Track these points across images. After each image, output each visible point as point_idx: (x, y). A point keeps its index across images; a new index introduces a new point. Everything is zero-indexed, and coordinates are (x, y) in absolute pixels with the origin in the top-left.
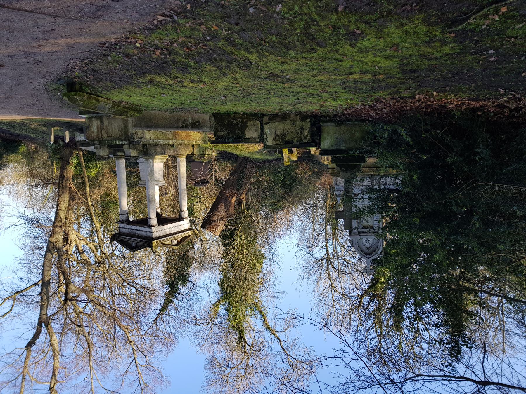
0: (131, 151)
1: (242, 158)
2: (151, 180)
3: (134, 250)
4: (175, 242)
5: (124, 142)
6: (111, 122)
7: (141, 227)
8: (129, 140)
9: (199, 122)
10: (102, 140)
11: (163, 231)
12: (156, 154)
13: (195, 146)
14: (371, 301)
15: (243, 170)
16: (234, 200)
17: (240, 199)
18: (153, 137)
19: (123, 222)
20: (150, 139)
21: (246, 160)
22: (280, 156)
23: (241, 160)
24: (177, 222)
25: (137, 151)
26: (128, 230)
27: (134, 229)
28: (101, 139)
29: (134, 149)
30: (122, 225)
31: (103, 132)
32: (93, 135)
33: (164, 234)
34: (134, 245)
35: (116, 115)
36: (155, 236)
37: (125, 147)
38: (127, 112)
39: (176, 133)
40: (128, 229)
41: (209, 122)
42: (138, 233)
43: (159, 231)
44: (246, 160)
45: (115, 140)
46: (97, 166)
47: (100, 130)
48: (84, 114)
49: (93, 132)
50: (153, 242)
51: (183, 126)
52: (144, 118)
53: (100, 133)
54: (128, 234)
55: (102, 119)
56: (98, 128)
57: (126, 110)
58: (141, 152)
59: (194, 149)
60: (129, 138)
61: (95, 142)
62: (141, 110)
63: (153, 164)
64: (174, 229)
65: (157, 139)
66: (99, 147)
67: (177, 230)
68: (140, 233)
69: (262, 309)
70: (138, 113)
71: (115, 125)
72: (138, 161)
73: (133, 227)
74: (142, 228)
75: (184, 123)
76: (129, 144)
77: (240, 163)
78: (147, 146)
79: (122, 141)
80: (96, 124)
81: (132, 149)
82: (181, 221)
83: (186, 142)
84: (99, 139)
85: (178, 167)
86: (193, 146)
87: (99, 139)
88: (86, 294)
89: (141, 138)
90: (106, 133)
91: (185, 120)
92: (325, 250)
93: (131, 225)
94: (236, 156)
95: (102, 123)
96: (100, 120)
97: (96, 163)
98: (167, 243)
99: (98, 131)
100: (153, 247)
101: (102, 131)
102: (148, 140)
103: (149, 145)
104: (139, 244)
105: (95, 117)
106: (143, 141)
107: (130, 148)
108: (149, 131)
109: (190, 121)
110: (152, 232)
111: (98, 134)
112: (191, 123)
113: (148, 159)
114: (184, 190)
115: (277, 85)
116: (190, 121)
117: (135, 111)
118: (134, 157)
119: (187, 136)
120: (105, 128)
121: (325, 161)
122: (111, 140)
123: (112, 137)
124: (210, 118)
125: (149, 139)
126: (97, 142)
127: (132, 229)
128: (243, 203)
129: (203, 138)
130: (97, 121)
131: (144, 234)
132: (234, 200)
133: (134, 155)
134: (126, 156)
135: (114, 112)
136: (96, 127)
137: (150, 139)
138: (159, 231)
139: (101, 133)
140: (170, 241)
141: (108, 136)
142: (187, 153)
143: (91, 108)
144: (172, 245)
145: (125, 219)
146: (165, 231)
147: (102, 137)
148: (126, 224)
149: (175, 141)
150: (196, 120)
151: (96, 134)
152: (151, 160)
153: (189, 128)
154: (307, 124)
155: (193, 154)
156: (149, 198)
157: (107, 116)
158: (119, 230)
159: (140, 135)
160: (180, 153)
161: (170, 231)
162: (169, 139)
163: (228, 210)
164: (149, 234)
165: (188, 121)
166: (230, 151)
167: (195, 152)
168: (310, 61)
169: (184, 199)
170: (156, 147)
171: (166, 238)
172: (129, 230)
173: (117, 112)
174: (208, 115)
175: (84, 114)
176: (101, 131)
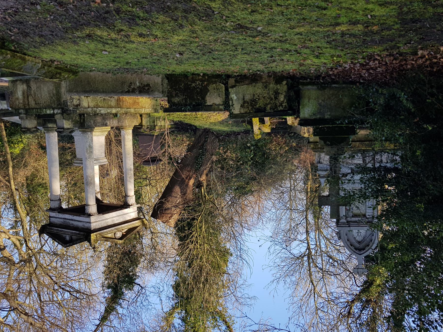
0: (64, 121)
1: (202, 131)
2: (89, 158)
3: (68, 245)
4: (119, 235)
5: (56, 111)
6: (40, 86)
7: (77, 216)
8: (62, 109)
9: (148, 85)
10: (29, 109)
11: (104, 221)
12: (96, 126)
13: (144, 116)
14: (363, 308)
15: (203, 145)
16: (192, 182)
17: (199, 181)
18: (91, 105)
19: (55, 210)
20: (89, 107)
21: (207, 132)
22: (249, 127)
23: (200, 133)
24: (121, 209)
25: (72, 121)
26: (60, 220)
27: (68, 219)
29: (68, 120)
30: (53, 214)
33: (105, 225)
34: (68, 238)
35: (46, 77)
36: (94, 228)
37: (57, 117)
38: (60, 74)
39: (120, 99)
40: (61, 218)
41: (161, 86)
42: (72, 224)
43: (99, 221)
44: (207, 132)
46: (22, 141)
47: (26, 97)
48: (6, 77)
50: (92, 235)
51: (129, 90)
52: (81, 81)
53: (26, 100)
54: (60, 225)
55: (29, 83)
56: (23, 93)
57: (59, 71)
58: (77, 123)
59: (143, 119)
60: (63, 106)
62: (77, 71)
63: (92, 138)
64: (117, 218)
65: (97, 106)
66: (25, 118)
67: (121, 220)
68: (76, 223)
69: (227, 319)
70: (73, 75)
71: (45, 89)
72: (73, 134)
73: (67, 216)
74: (78, 217)
75: (130, 86)
76: (62, 114)
77: (200, 136)
78: (84, 116)
79: (54, 109)
80: (21, 89)
81: (66, 119)
82: (126, 208)
83: (132, 110)
84: (25, 107)
85: (122, 141)
86: (141, 116)
87: (25, 107)
88: (8, 300)
89: (77, 105)
90: (34, 100)
91: (131, 83)
92: (306, 245)
93: (64, 214)
94: (194, 128)
95: (29, 87)
96: (27, 84)
97: (21, 137)
98: (109, 235)
99: (24, 97)
100: (92, 241)
101: (29, 98)
102: (86, 108)
103: (87, 114)
104: (74, 237)
105: (21, 80)
106: (80, 109)
107: (63, 118)
108: (87, 97)
109: (138, 84)
110: (90, 223)
111: (24, 101)
112: (140, 86)
113: (85, 132)
114: (131, 170)
115: (245, 39)
116: (138, 84)
117: (69, 72)
118: (68, 129)
119: (134, 103)
120: (32, 93)
121: (305, 133)
122: (40, 109)
123: (41, 105)
124: (162, 81)
125: (87, 107)
126: (22, 111)
127: (65, 219)
128: (203, 186)
129: (153, 105)
130: (23, 84)
131: (80, 225)
132: (192, 182)
133: (69, 127)
134: (58, 129)
135: (45, 74)
136: (21, 92)
137: (89, 107)
138: (99, 221)
139: (28, 101)
140: (113, 234)
141: (36, 104)
142: (134, 125)
143: (16, 69)
144: (116, 239)
145: (57, 206)
146: (107, 221)
147: (28, 105)
148: (59, 212)
149: (120, 109)
150: (146, 84)
151: (21, 102)
152: (89, 133)
153: (137, 93)
154: (283, 87)
155: (141, 125)
156: (86, 180)
157: (35, 79)
158: (50, 220)
159: (75, 102)
160: (125, 124)
161: (113, 221)
162: (112, 107)
163: (184, 194)
164: (87, 225)
165: (135, 84)
166: (187, 121)
167: (144, 123)
168: (287, 9)
169: (130, 182)
170: (95, 117)
171: (108, 230)
172: (62, 220)
173: (48, 74)
174: (161, 76)
175: (7, 76)
176: (28, 97)
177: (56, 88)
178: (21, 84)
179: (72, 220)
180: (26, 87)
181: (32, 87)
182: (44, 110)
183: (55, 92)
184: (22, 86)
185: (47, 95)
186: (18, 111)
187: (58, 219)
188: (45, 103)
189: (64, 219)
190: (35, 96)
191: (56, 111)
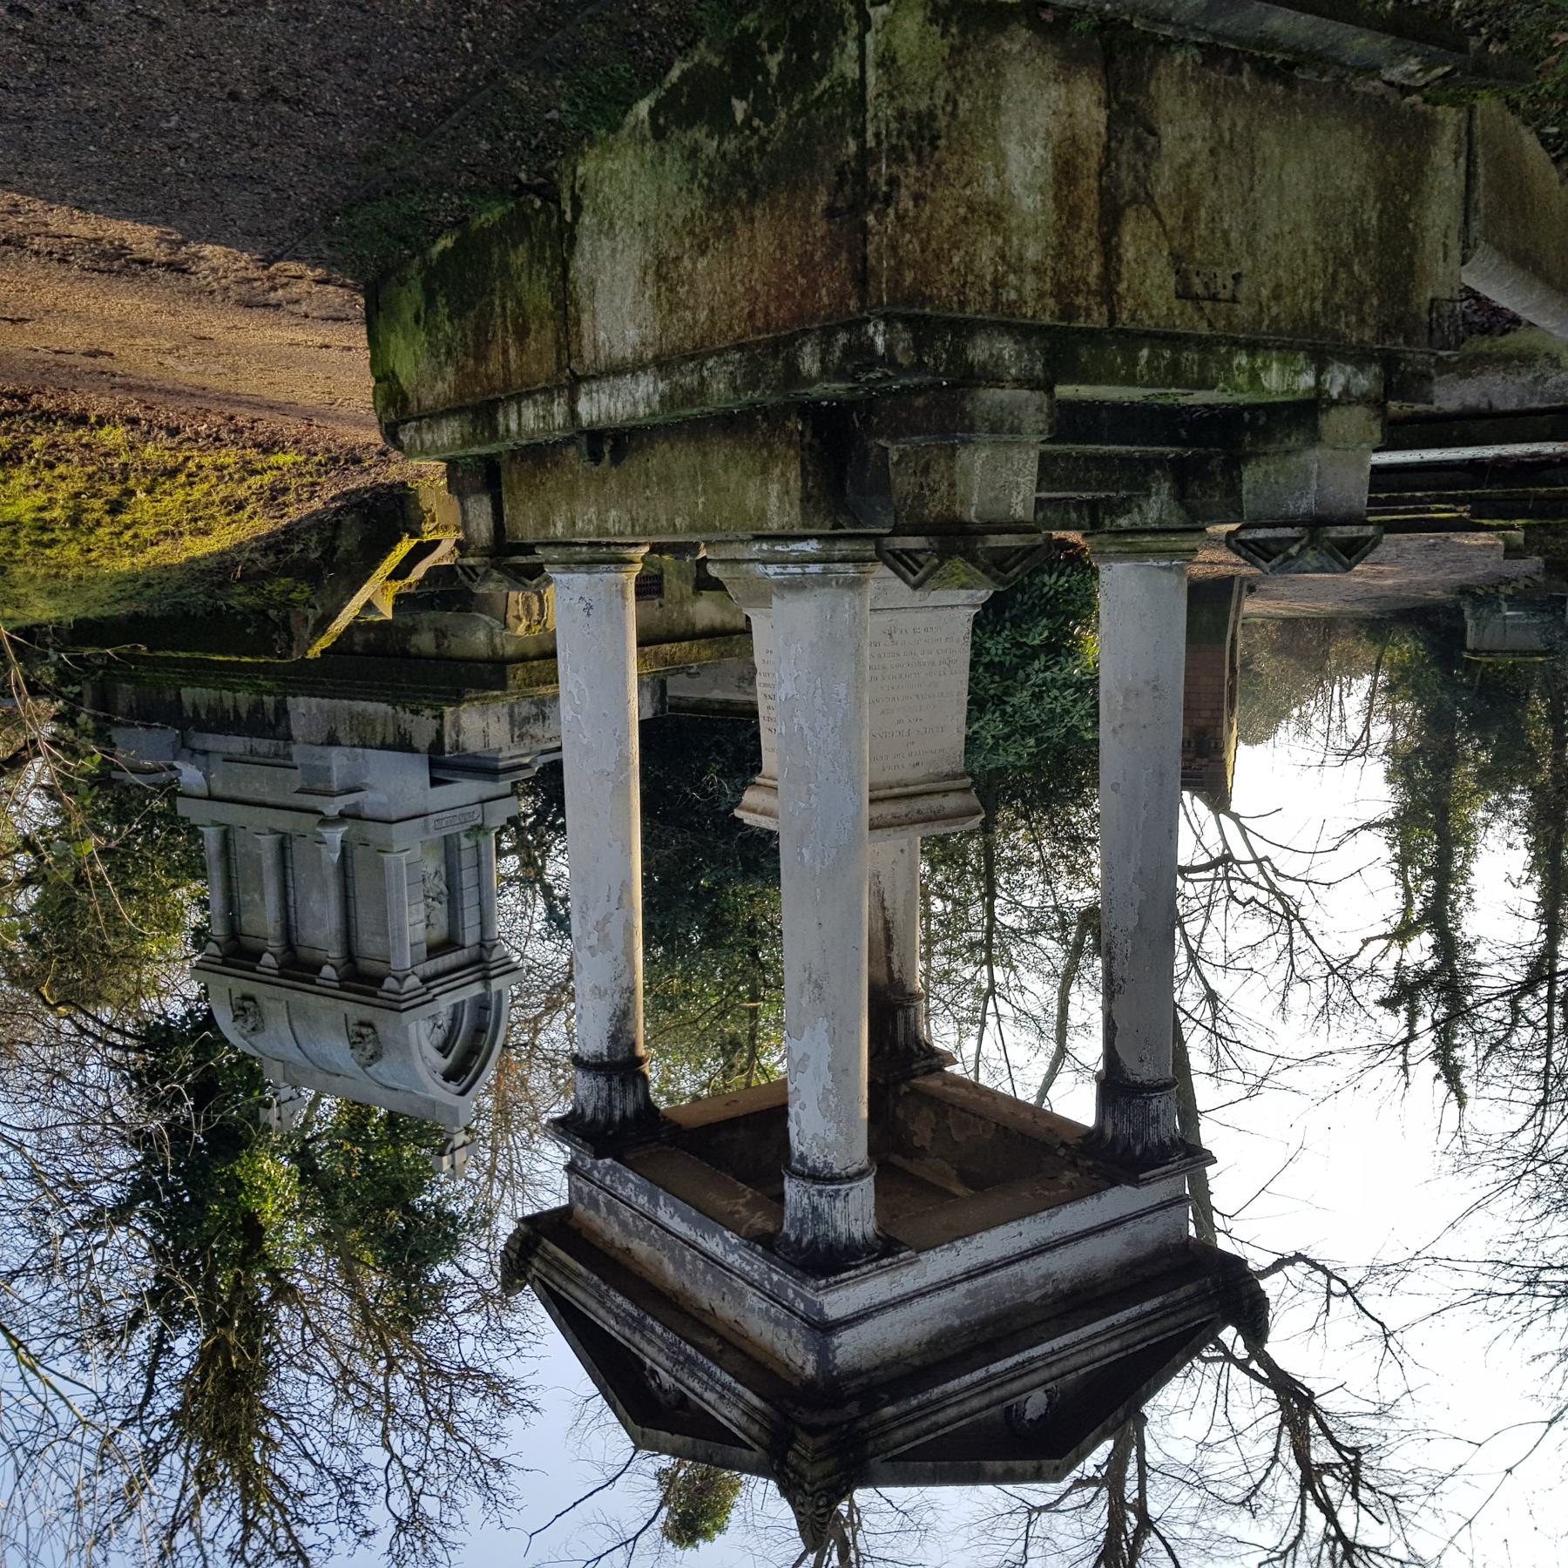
28: (1099, 319)
31: (1134, 238)
32: (986, 255)
45: (1252, 348)
47: (1091, 207)
49: (994, 215)
53: (1086, 245)
56: (1065, 172)
61: (980, 351)
80: (1041, 119)
90: (1176, 258)
99: (1069, 213)
111: (1063, 250)
120: (1164, 185)
126: (1007, 348)
136: (1039, 152)
139: (1110, 252)
141: (1184, 293)
147: (1108, 292)
151: (1033, 252)
176: (1111, 218)
177: (1386, 192)
178: (1049, 65)
181: (1169, 133)
182: (1242, 359)
183: (1371, 216)
184: (1055, 92)
185: (1308, 233)
186: (957, 353)
187: (922, 1306)
188: (1276, 296)
189: (969, 1275)
190: (1188, 219)
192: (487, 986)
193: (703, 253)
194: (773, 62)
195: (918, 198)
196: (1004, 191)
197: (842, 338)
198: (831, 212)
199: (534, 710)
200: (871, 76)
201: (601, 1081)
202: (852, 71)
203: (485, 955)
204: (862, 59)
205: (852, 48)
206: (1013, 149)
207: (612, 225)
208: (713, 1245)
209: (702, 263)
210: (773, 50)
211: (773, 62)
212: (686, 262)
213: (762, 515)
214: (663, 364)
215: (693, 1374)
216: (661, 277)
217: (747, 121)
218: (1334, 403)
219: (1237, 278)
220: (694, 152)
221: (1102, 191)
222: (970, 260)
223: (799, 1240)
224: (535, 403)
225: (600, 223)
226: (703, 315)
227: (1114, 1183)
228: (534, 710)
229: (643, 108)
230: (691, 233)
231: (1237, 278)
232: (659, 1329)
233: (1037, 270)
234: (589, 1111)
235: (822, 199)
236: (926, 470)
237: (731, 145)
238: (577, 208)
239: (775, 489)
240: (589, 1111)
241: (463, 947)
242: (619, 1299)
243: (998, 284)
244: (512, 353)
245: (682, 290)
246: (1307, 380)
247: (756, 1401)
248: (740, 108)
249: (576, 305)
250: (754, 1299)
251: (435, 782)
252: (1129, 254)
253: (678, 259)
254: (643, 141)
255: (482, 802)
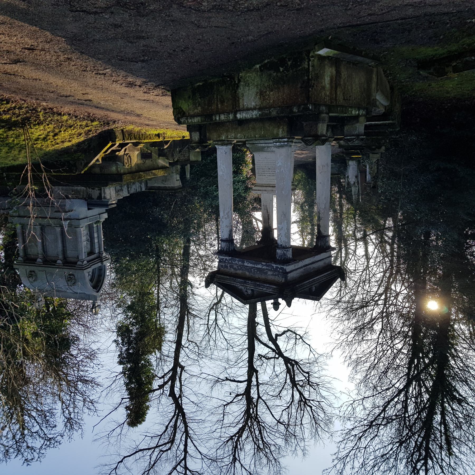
28: (334, 104)
45: (351, 107)
47: (334, 85)
49: (324, 88)
80: (329, 74)
90: (343, 94)
95: (338, 72)
99: (331, 87)
101: (338, 89)
120: (342, 83)
130: (332, 67)
136: (329, 78)
139: (336, 94)
147: (336, 100)
151: (328, 93)
179: (313, 263)
180: (335, 72)
181: (343, 74)
182: (350, 109)
183: (365, 86)
184: (331, 69)
185: (358, 89)
186: (319, 109)
187: (298, 271)
189: (304, 266)
190: (345, 87)
191: (361, 112)
192: (102, 264)
193: (272, 91)
194: (289, 63)
195: (316, 86)
196: (325, 84)
197: (302, 106)
198: (301, 87)
199: (120, 188)
200: (311, 68)
201: (228, 243)
202: (307, 67)
203: (101, 255)
204: (309, 65)
205: (306, 63)
206: (326, 78)
207: (249, 84)
208: (259, 266)
209: (271, 93)
210: (289, 61)
211: (289, 63)
212: (268, 92)
213: (278, 134)
214: (260, 109)
215: (259, 287)
216: (261, 94)
217: (283, 71)
218: (360, 116)
219: (350, 96)
220: (270, 75)
221: (335, 84)
222: (322, 95)
223: (281, 259)
224: (224, 115)
225: (246, 84)
226: (271, 101)
227: (322, 253)
228: (120, 188)
229: (258, 66)
230: (269, 88)
231: (350, 96)
232: (250, 282)
233: (328, 96)
234: (225, 249)
235: (299, 85)
236: (311, 127)
237: (279, 74)
238: (239, 81)
239: (281, 130)
240: (225, 249)
241: (95, 254)
242: (239, 280)
243: (324, 98)
244: (219, 105)
245: (267, 97)
246: (357, 112)
247: (275, 287)
248: (281, 69)
249: (238, 98)
250: (269, 273)
251: (89, 209)
252: (338, 93)
253: (265, 92)
254: (258, 71)
255: (99, 214)
